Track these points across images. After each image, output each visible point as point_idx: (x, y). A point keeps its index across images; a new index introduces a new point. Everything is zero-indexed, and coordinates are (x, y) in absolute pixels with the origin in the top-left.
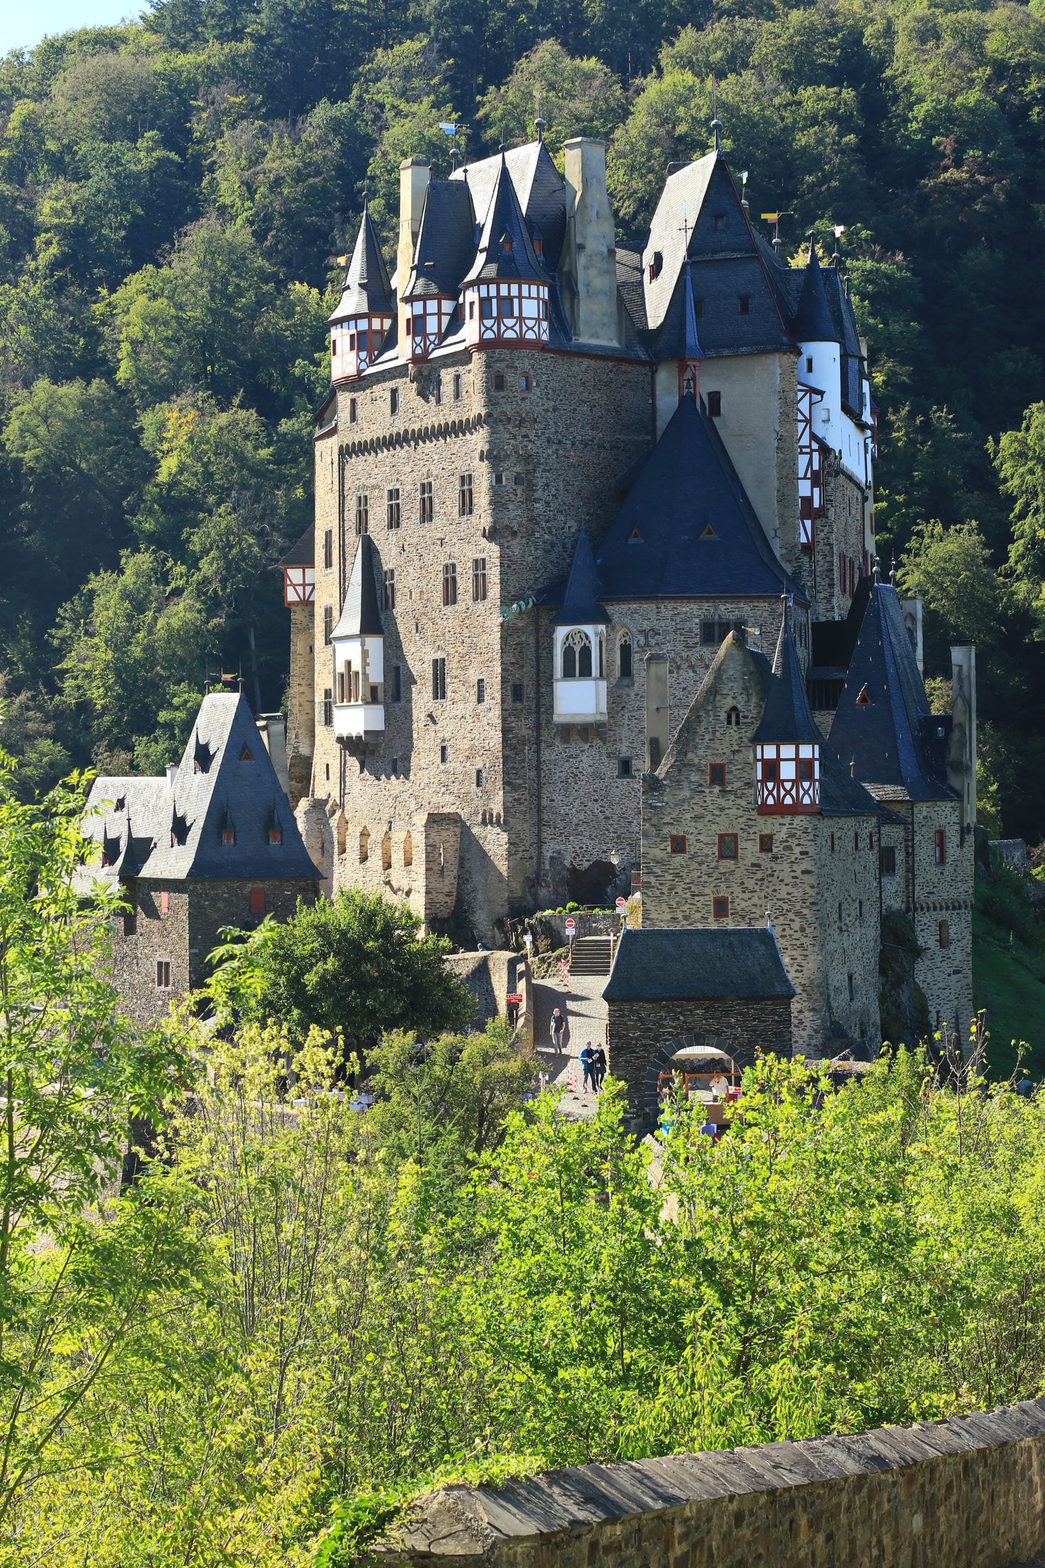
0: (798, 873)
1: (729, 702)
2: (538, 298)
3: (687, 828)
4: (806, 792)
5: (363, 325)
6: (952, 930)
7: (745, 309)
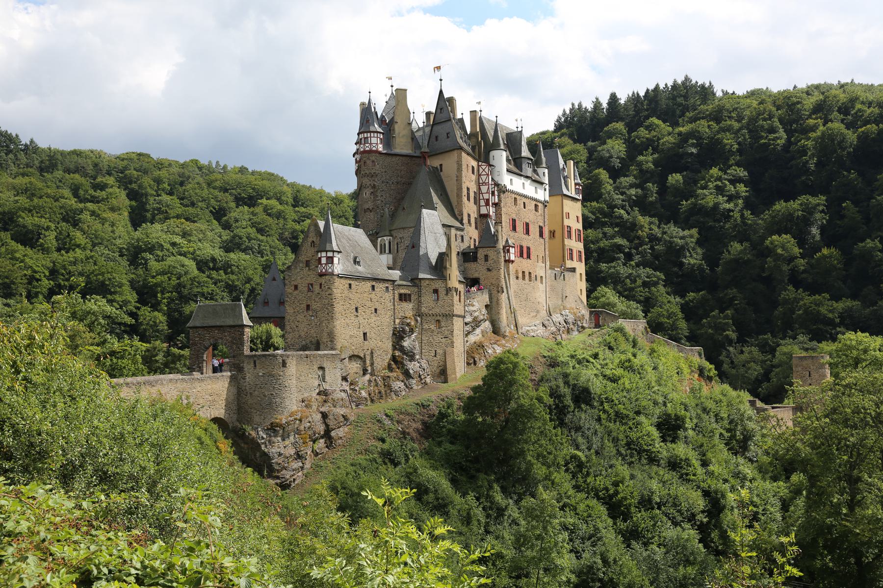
1: (310, 240)
2: (377, 137)
3: (298, 281)
4: (330, 268)
6: (443, 324)
7: (448, 137)
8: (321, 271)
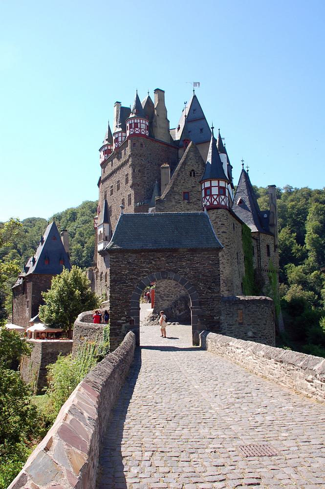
0: (220, 233)
4: (223, 200)
5: (106, 148)
8: (211, 204)
